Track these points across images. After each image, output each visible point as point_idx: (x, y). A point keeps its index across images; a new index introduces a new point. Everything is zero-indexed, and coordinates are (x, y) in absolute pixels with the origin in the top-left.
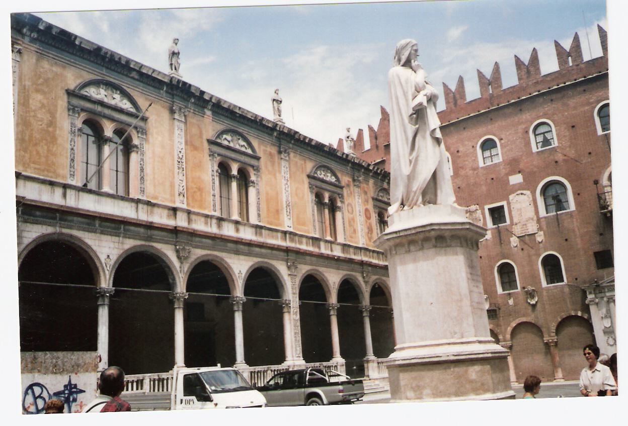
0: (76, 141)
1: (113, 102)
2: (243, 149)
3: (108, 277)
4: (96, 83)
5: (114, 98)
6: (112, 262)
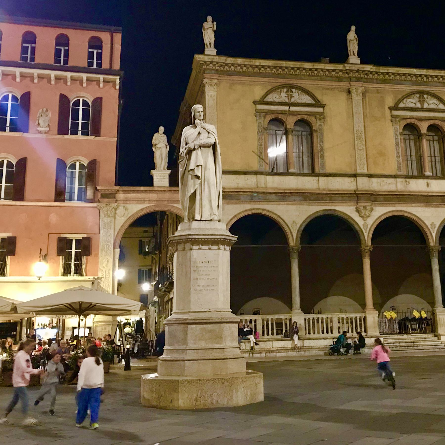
1: (293, 100)
2: (433, 106)
3: (295, 237)
6: (298, 226)
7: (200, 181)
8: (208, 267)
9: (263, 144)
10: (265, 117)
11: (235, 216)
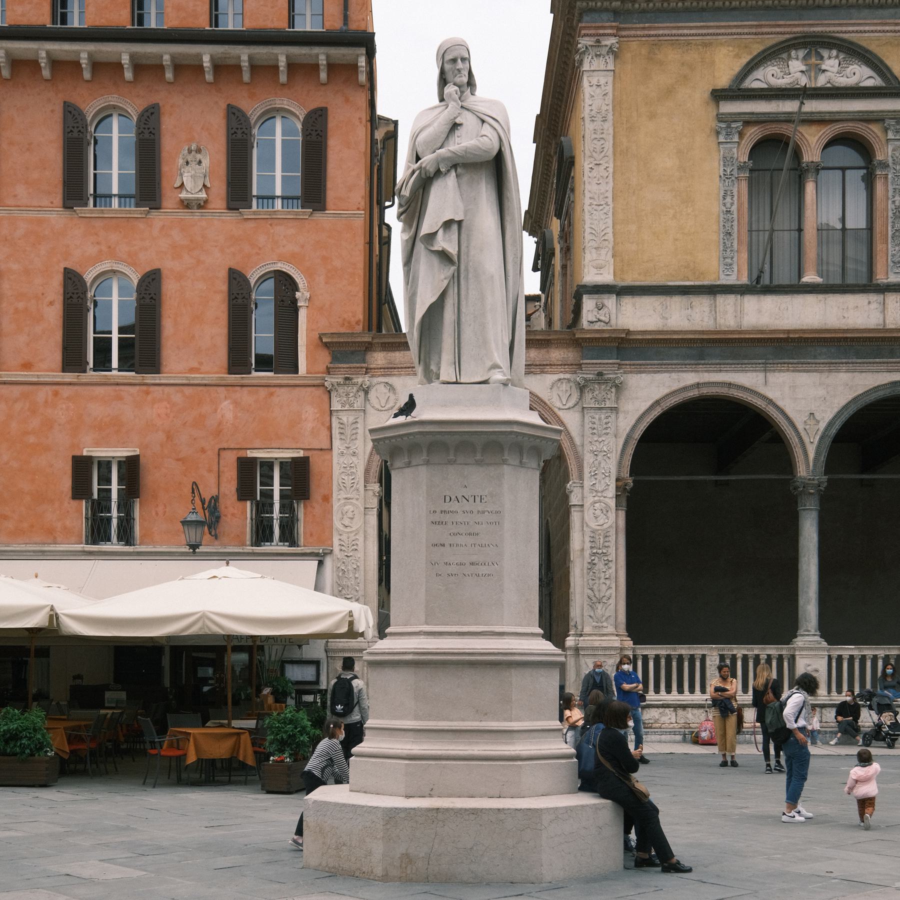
0: (735, 193)
1: (821, 81)
4: (774, 53)
5: (824, 71)
7: (453, 268)
8: (472, 512)
9: (734, 208)
10: (741, 135)
11: (657, 403)
